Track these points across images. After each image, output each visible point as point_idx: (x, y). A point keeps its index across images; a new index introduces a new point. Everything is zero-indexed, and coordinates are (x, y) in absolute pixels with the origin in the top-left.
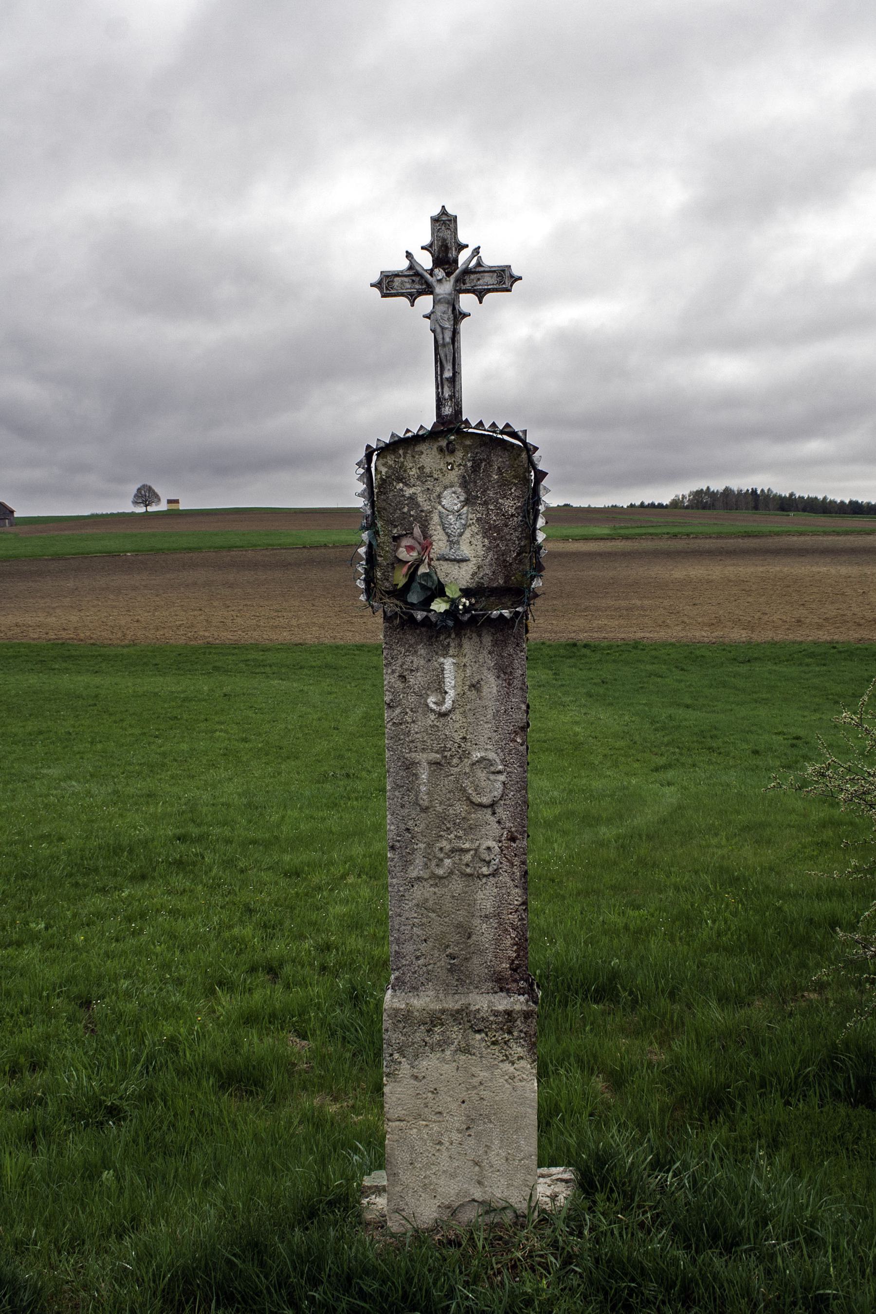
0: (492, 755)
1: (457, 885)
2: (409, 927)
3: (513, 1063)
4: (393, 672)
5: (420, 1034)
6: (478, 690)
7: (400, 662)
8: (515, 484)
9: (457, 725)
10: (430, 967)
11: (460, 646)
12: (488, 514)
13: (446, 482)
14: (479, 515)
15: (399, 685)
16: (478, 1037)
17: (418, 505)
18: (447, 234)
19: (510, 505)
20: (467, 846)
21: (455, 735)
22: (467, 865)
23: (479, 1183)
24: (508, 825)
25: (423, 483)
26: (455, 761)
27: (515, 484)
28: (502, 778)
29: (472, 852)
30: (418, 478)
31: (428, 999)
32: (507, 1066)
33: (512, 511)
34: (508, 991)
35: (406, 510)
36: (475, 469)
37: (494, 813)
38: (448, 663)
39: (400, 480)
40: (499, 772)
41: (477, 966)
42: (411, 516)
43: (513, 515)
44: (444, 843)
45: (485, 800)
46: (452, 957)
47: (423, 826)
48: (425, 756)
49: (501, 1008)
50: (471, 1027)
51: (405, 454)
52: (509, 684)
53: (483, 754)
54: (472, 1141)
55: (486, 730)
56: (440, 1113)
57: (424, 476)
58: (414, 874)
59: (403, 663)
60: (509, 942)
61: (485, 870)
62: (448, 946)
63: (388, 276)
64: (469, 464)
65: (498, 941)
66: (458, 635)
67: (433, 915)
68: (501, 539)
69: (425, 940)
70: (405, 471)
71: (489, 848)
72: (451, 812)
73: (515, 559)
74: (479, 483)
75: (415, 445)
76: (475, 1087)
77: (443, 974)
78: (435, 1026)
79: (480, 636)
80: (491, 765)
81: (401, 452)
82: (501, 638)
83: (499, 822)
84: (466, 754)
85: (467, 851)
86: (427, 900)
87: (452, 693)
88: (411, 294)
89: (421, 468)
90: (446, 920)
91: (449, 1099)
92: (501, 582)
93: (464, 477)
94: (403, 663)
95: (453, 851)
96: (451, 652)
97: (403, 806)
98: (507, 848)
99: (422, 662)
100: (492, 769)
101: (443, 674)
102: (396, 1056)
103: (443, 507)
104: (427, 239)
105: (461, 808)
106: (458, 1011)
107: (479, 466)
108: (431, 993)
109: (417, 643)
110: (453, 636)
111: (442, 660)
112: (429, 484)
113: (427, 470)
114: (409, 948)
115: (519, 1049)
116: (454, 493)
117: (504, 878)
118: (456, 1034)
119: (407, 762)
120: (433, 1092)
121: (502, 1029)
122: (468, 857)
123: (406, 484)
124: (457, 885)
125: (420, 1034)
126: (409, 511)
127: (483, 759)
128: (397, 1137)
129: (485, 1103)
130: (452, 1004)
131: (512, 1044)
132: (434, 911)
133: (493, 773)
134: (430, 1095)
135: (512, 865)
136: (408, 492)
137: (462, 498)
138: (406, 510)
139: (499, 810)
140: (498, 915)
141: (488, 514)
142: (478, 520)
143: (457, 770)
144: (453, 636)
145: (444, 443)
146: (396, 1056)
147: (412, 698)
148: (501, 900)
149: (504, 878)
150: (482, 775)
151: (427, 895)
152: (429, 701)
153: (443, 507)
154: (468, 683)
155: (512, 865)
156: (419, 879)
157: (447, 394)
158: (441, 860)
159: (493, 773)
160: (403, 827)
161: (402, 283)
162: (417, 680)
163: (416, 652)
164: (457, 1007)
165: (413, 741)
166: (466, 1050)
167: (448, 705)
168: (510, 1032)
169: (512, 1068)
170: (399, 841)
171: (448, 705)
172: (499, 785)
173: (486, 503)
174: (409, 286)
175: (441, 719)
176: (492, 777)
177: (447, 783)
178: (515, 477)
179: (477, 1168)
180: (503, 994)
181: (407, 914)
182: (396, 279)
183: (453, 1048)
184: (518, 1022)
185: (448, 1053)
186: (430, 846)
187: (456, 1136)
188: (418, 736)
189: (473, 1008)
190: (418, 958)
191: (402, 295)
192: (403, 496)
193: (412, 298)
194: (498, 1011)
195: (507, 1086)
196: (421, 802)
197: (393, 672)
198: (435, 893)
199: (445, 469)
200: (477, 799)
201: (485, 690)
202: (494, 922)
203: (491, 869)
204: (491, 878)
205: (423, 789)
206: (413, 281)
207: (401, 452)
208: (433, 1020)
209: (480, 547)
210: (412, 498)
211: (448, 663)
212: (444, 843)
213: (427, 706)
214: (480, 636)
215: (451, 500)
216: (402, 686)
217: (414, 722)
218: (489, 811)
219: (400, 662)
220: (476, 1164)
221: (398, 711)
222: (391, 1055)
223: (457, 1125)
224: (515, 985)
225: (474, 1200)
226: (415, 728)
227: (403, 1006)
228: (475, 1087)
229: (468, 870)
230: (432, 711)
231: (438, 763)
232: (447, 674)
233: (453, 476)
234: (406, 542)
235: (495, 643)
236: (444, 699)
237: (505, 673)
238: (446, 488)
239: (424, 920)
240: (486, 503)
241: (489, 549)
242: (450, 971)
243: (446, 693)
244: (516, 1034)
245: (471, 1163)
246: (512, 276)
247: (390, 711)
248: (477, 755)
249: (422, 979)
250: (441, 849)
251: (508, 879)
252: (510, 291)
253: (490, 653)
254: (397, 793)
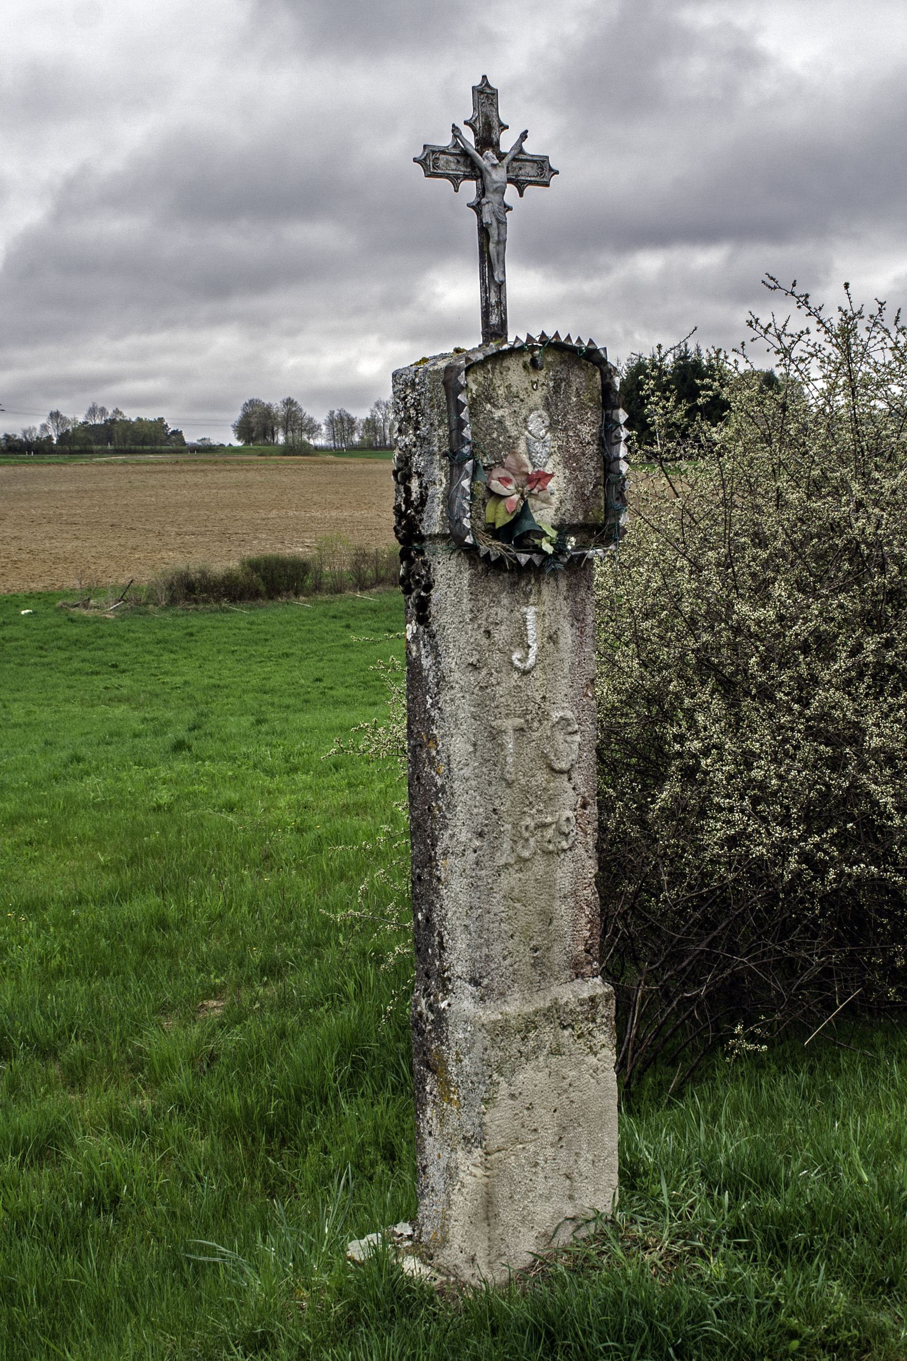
0: (569, 715)
1: (539, 867)
2: (497, 924)
3: (595, 1054)
4: (479, 627)
5: (516, 1044)
6: (555, 642)
7: (485, 615)
8: (591, 408)
9: (538, 683)
10: (516, 966)
11: (539, 592)
12: (568, 442)
13: (531, 404)
14: (560, 443)
15: (484, 642)
16: (566, 1033)
17: (505, 430)
18: (488, 109)
19: (587, 431)
20: (549, 819)
21: (536, 694)
22: (550, 842)
23: (571, 1197)
24: (583, 789)
25: (510, 404)
26: (536, 724)
27: (591, 408)
28: (577, 738)
29: (554, 826)
30: (506, 398)
31: (518, 1003)
32: (592, 1060)
33: (588, 438)
34: (583, 976)
35: (495, 435)
36: (556, 389)
37: (570, 779)
38: (530, 612)
39: (489, 399)
40: (576, 732)
41: (558, 956)
42: (500, 442)
43: (589, 443)
44: (528, 821)
45: (564, 765)
46: (535, 949)
47: (509, 803)
48: (510, 722)
49: (586, 995)
50: (560, 1024)
51: (493, 368)
52: (582, 633)
53: (562, 714)
54: (563, 1153)
55: (563, 686)
56: (535, 1130)
57: (512, 397)
58: (502, 862)
59: (488, 616)
60: (584, 921)
61: (565, 845)
62: (531, 938)
63: (434, 152)
64: (551, 384)
65: (575, 922)
66: (538, 580)
67: (518, 905)
68: (580, 469)
69: (512, 936)
70: (494, 389)
71: (568, 819)
72: (534, 783)
73: (591, 492)
74: (560, 406)
75: (503, 359)
76: (565, 1091)
77: (527, 970)
78: (529, 1031)
79: (556, 580)
80: (569, 725)
81: (489, 366)
82: (575, 581)
83: (574, 789)
84: (546, 716)
85: (551, 824)
86: (513, 889)
87: (535, 647)
88: (457, 177)
89: (509, 387)
90: (531, 908)
91: (544, 1111)
92: (581, 517)
93: (547, 399)
94: (488, 616)
95: (537, 827)
96: (531, 600)
97: (490, 784)
98: (581, 816)
99: (506, 613)
100: (570, 729)
101: (525, 625)
102: (495, 1076)
103: (530, 432)
104: (469, 114)
105: (541, 777)
106: (549, 1009)
107: (559, 386)
108: (517, 996)
109: (501, 592)
110: (533, 581)
111: (524, 609)
112: (516, 406)
113: (514, 389)
114: (497, 948)
115: (602, 1037)
116: (540, 416)
117: (580, 850)
118: (548, 1034)
119: (494, 732)
120: (528, 1109)
121: (587, 1019)
122: (550, 833)
123: (494, 406)
124: (539, 867)
125: (516, 1044)
126: (499, 436)
127: (562, 718)
128: (496, 1171)
129: (574, 1106)
130: (542, 1002)
131: (596, 1033)
132: (519, 901)
133: (570, 733)
134: (525, 1112)
135: (586, 833)
136: (497, 414)
137: (547, 423)
138: (495, 435)
139: (574, 775)
140: (574, 893)
141: (568, 442)
142: (560, 447)
143: (537, 734)
144: (533, 581)
145: (528, 358)
146: (495, 1076)
147: (497, 656)
148: (577, 875)
149: (580, 850)
150: (560, 737)
151: (513, 883)
152: (514, 657)
153: (530, 432)
154: (547, 634)
155: (586, 833)
156: (506, 866)
157: (493, 300)
158: (527, 840)
159: (570, 733)
160: (490, 807)
161: (447, 162)
162: (501, 634)
163: (499, 602)
164: (548, 1004)
165: (497, 707)
166: (556, 1052)
167: (531, 660)
168: (594, 1021)
169: (595, 1060)
170: (486, 825)
171: (531, 660)
172: (575, 747)
173: (565, 429)
174: (454, 167)
175: (524, 678)
176: (569, 738)
177: (530, 751)
178: (591, 400)
179: (568, 1181)
180: (579, 980)
181: (495, 910)
182: (442, 156)
183: (545, 1052)
184: (600, 1007)
185: (541, 1059)
186: (515, 825)
187: (550, 1152)
188: (503, 700)
189: (562, 1002)
190: (504, 958)
191: (447, 176)
192: (493, 419)
193: (455, 180)
194: (584, 1000)
195: (592, 1081)
196: (508, 776)
197: (479, 627)
198: (520, 879)
199: (530, 388)
200: (558, 766)
201: (562, 641)
202: (571, 901)
203: (570, 842)
204: (569, 852)
205: (510, 760)
206: (458, 162)
207: (489, 366)
208: (529, 1025)
209: (561, 479)
210: (500, 422)
211: (530, 612)
212: (528, 821)
213: (512, 663)
214: (556, 580)
215: (537, 424)
216: (487, 642)
217: (498, 684)
218: (565, 777)
219: (485, 615)
220: (568, 1177)
221: (484, 672)
222: (490, 1076)
223: (551, 1139)
224: (589, 968)
225: (567, 1219)
226: (500, 690)
227: (500, 1017)
228: (565, 1091)
229: (551, 847)
230: (517, 669)
231: (522, 729)
232: (530, 626)
233: (537, 397)
234: (498, 473)
235: (570, 588)
236: (527, 654)
237: (578, 620)
238: (531, 411)
239: (511, 913)
240: (565, 429)
241: (570, 481)
242: (533, 966)
243: (529, 647)
244: (598, 1020)
245: (563, 1178)
246: (551, 169)
247: (476, 673)
248: (556, 715)
249: (509, 982)
250: (527, 828)
251: (583, 851)
252: (547, 185)
253: (565, 599)
254: (484, 770)
